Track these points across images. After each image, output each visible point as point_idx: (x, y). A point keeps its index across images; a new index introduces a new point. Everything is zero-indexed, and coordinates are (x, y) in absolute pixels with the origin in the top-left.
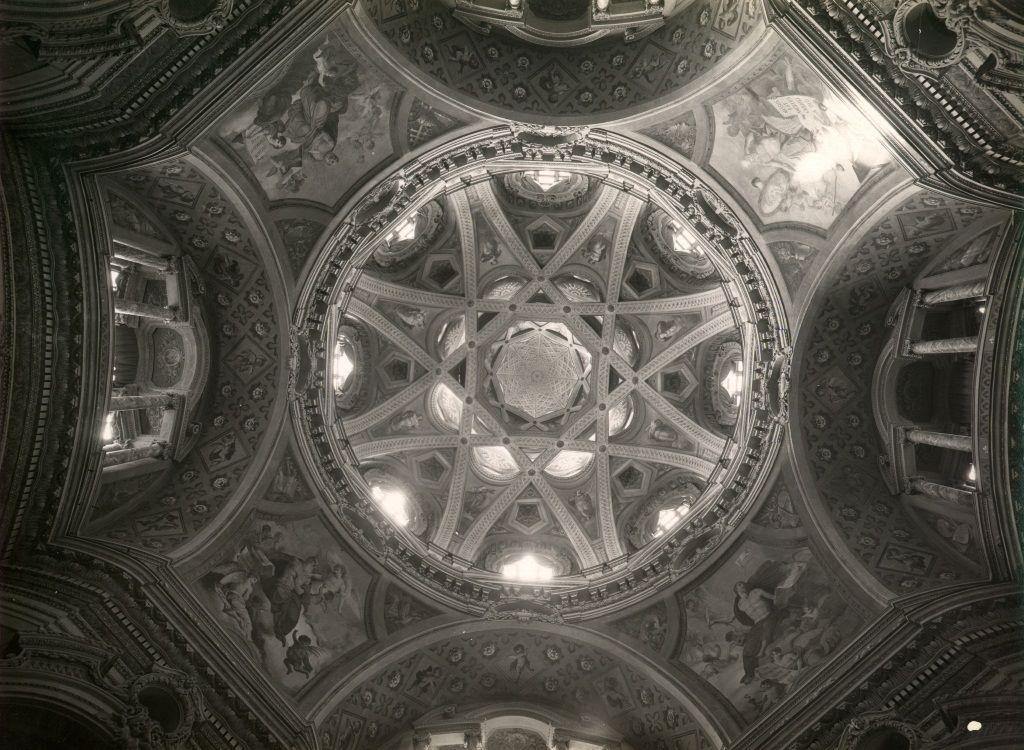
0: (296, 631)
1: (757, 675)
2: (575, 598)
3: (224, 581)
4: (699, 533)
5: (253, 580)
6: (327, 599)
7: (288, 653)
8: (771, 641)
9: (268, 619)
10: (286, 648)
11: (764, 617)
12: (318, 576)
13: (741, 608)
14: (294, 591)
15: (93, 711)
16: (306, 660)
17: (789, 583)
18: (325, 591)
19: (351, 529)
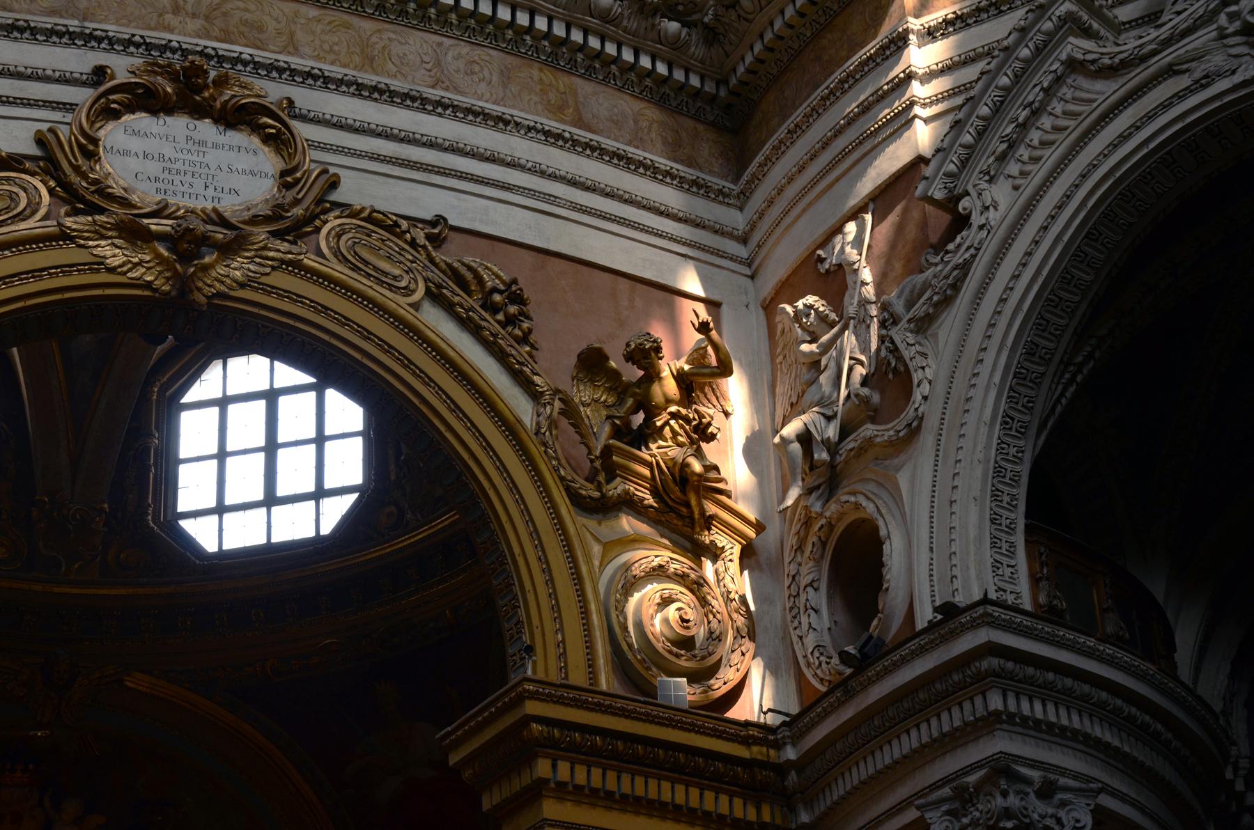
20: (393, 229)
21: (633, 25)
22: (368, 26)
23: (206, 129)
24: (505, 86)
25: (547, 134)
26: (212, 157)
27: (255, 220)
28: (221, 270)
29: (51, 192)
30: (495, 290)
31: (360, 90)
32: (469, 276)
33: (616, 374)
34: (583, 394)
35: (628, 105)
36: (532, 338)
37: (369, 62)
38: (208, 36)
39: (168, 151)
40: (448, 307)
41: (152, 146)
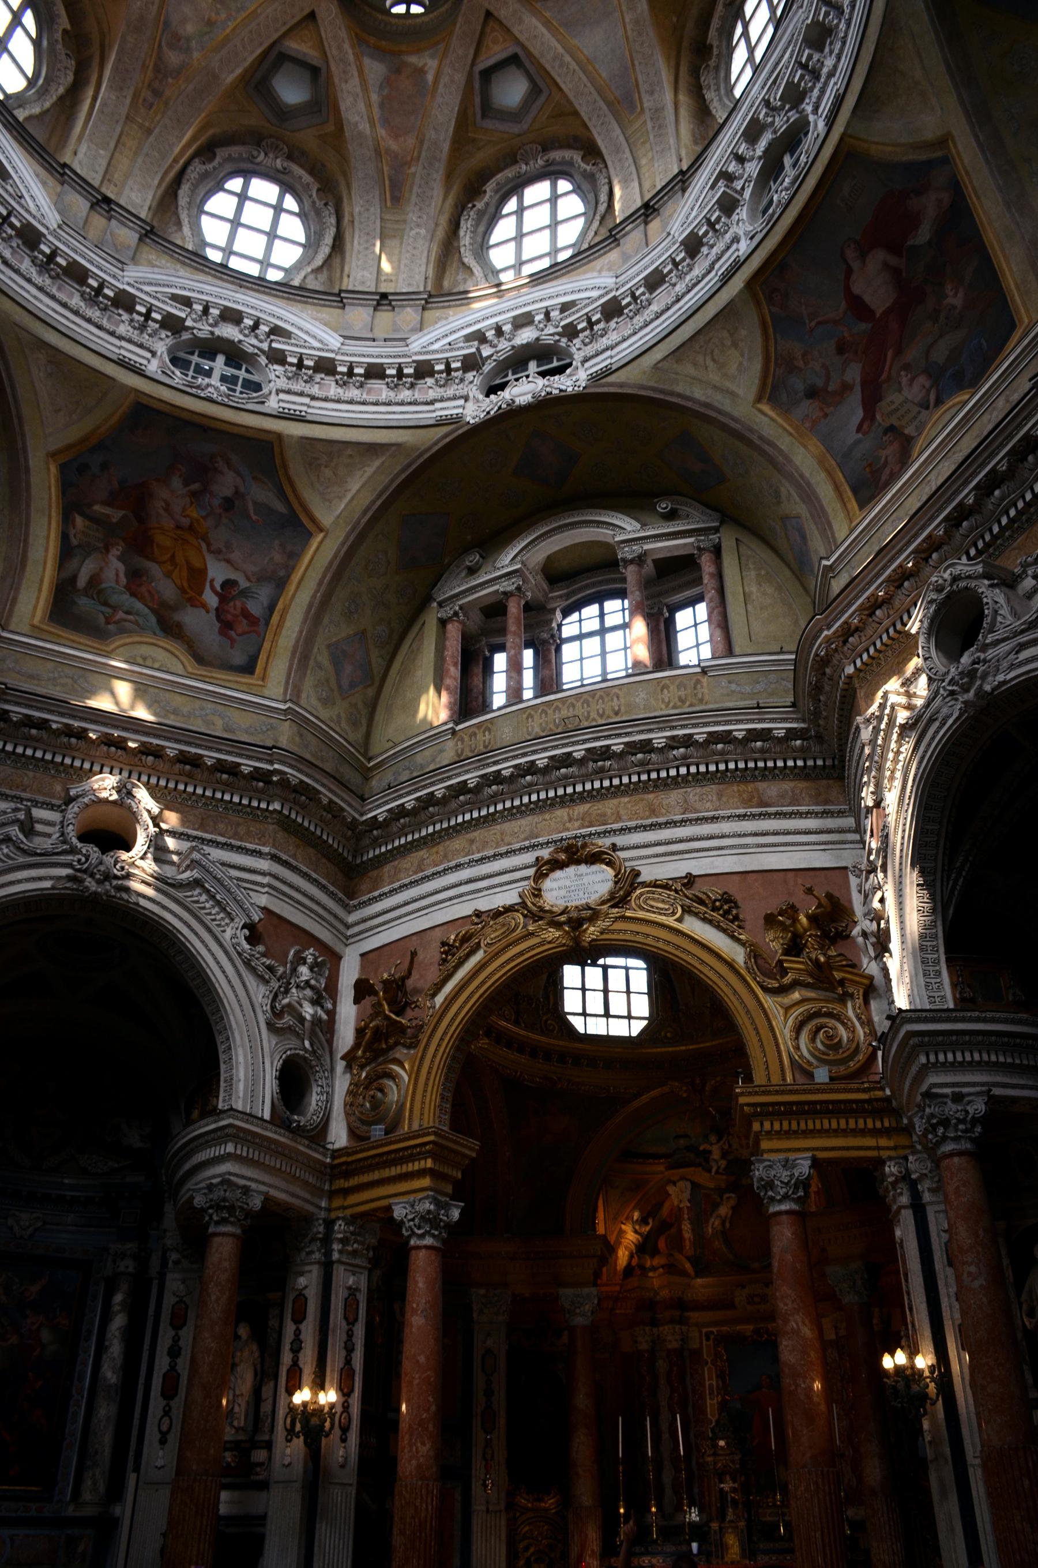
0: (212, 581)
1: (878, 417)
2: (598, 321)
3: (82, 582)
4: (781, 123)
5: (115, 552)
6: (227, 510)
7: (218, 617)
8: (899, 352)
9: (167, 589)
10: (213, 615)
11: (888, 304)
12: (196, 486)
13: (857, 289)
14: (178, 527)
15: (48, 884)
16: (246, 614)
17: (923, 235)
18: (216, 502)
19: (198, 387)
20: (666, 887)
21: (778, 749)
22: (651, 796)
23: (583, 868)
24: (719, 799)
25: (739, 816)
26: (586, 880)
27: (603, 903)
28: (592, 929)
29: (525, 916)
30: (716, 900)
31: (645, 828)
32: (704, 897)
33: (782, 923)
34: (770, 935)
35: (787, 786)
36: (741, 916)
37: (653, 812)
38: (583, 827)
39: (568, 883)
40: (696, 915)
41: (561, 883)
